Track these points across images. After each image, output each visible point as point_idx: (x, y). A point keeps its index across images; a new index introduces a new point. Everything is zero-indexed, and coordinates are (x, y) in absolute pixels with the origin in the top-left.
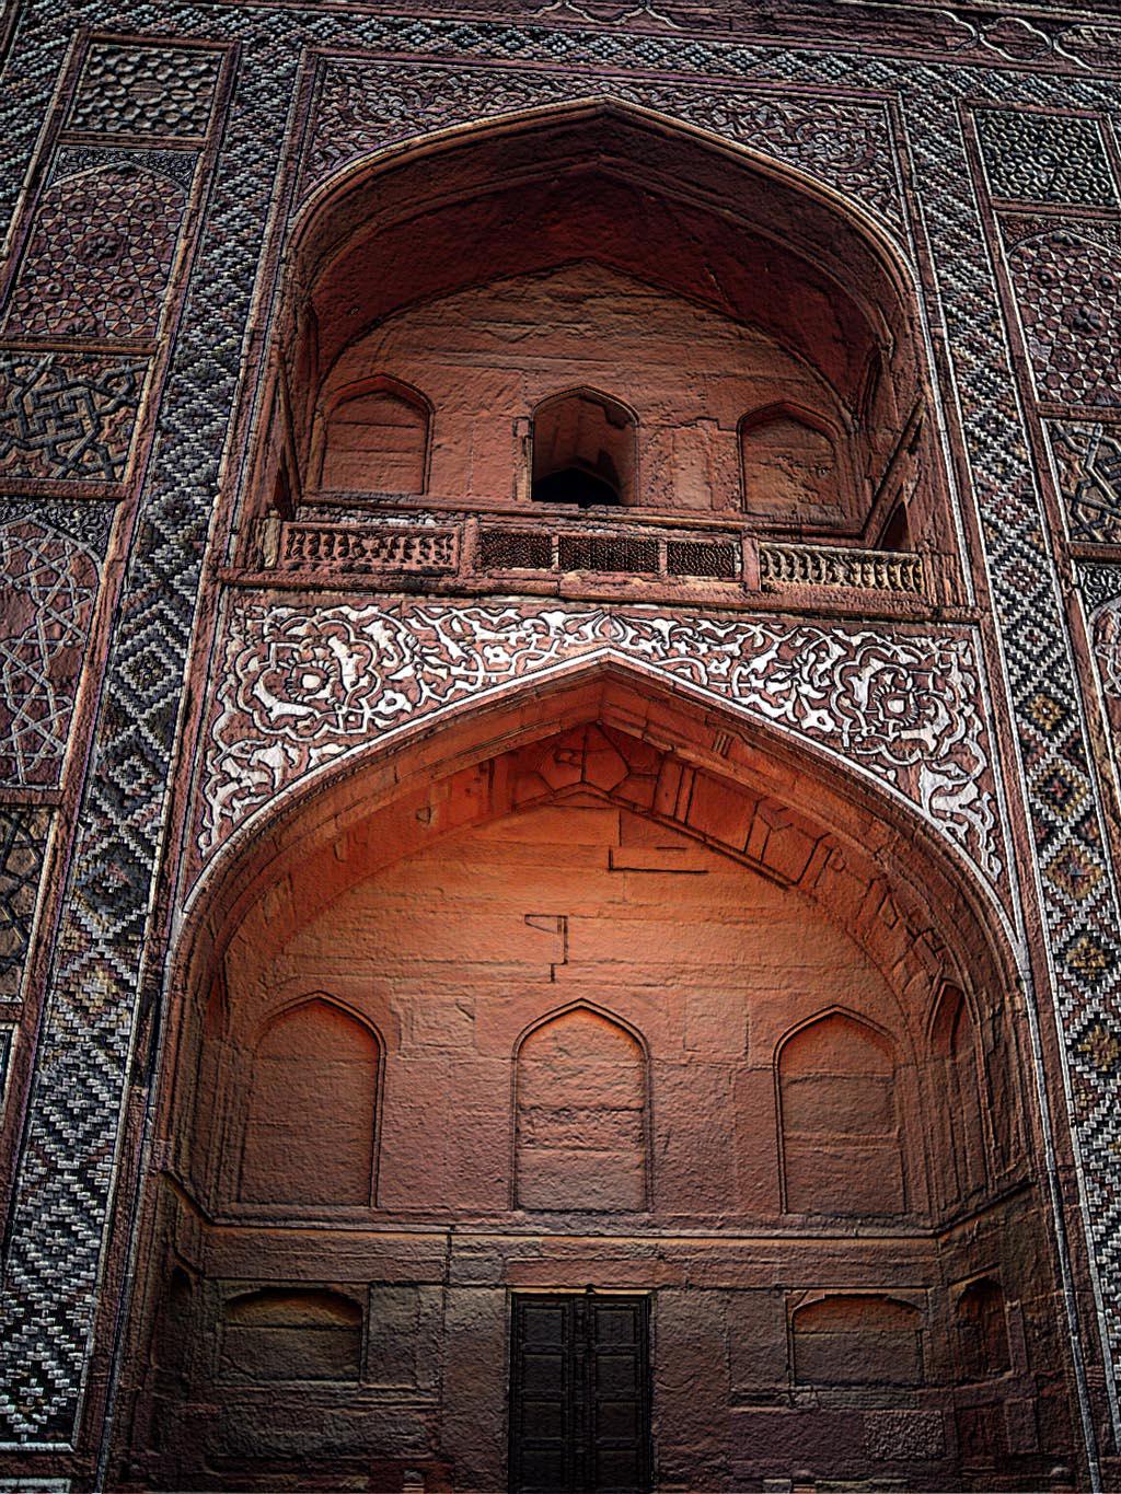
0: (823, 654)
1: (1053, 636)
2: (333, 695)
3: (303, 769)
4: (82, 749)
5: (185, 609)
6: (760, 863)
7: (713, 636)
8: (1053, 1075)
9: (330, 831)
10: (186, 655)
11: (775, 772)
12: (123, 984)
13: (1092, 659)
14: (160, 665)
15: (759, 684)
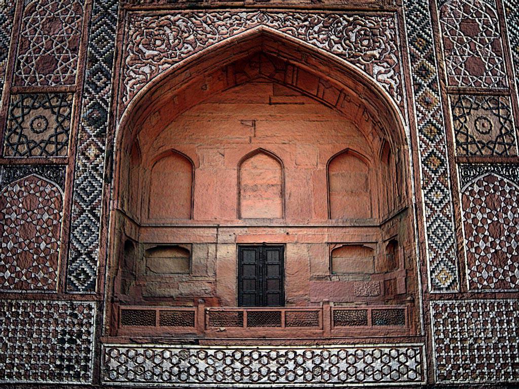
0: (339, 24)
1: (425, 15)
2: (166, 47)
3: (157, 73)
4: (82, 73)
5: (114, 20)
6: (323, 100)
7: (300, 19)
8: (416, 171)
9: (170, 95)
10: (115, 36)
11: (323, 68)
12: (102, 151)
13: (439, 23)
14: (106, 40)
15: (316, 36)
